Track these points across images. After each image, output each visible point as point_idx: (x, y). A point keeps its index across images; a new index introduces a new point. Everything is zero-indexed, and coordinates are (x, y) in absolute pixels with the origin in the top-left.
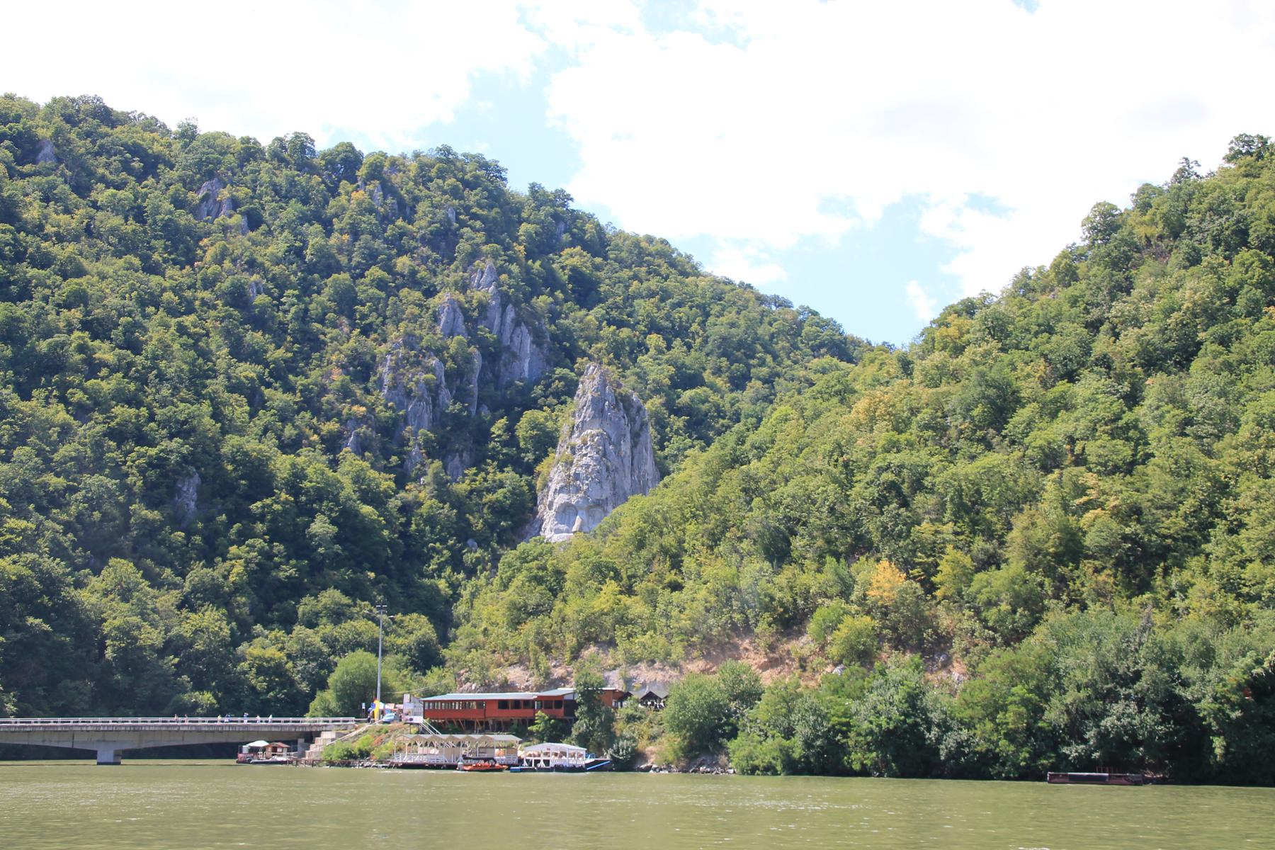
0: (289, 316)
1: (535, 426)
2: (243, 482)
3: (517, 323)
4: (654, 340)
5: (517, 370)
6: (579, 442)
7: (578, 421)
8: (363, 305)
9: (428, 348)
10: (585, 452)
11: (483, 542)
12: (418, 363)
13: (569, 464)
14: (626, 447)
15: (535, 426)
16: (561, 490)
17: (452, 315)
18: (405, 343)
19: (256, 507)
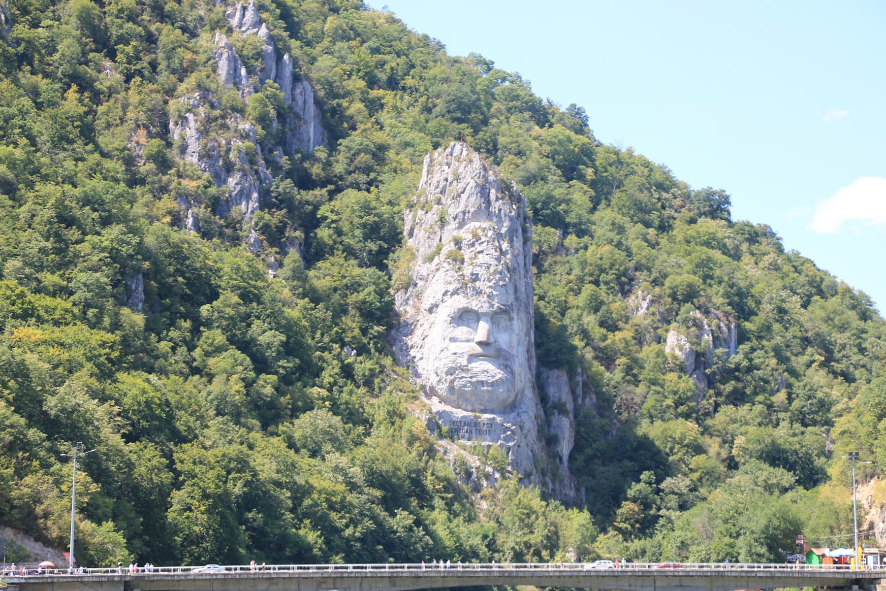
0: (56, 56)
1: (367, 209)
2: (181, 279)
3: (296, 78)
4: (389, 97)
5: (305, 135)
6: (465, 235)
7: (452, 211)
8: (127, 43)
9: (234, 109)
10: (479, 249)
11: (362, 350)
12: (225, 127)
13: (457, 260)
14: (518, 243)
15: (367, 209)
16: (455, 292)
17: (233, 63)
18: (204, 98)
19: (205, 310)
